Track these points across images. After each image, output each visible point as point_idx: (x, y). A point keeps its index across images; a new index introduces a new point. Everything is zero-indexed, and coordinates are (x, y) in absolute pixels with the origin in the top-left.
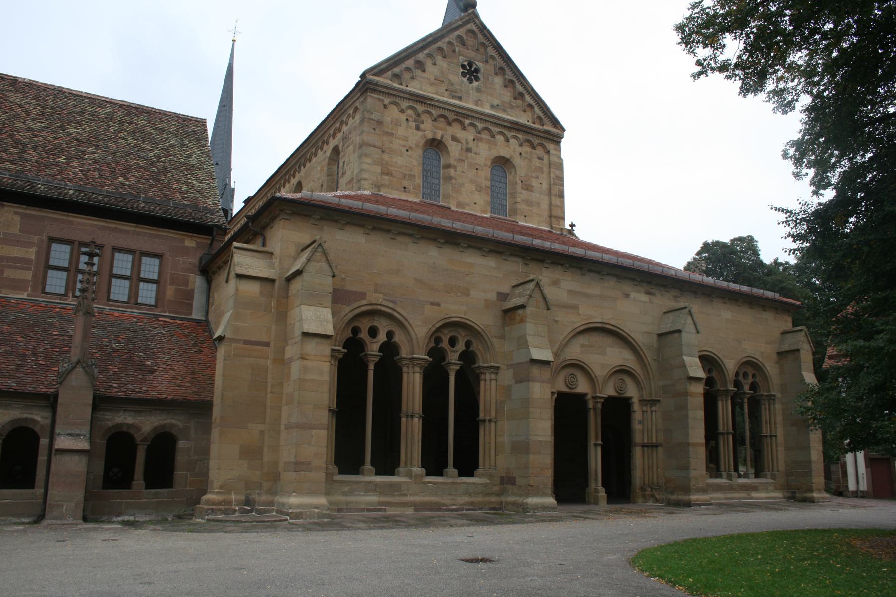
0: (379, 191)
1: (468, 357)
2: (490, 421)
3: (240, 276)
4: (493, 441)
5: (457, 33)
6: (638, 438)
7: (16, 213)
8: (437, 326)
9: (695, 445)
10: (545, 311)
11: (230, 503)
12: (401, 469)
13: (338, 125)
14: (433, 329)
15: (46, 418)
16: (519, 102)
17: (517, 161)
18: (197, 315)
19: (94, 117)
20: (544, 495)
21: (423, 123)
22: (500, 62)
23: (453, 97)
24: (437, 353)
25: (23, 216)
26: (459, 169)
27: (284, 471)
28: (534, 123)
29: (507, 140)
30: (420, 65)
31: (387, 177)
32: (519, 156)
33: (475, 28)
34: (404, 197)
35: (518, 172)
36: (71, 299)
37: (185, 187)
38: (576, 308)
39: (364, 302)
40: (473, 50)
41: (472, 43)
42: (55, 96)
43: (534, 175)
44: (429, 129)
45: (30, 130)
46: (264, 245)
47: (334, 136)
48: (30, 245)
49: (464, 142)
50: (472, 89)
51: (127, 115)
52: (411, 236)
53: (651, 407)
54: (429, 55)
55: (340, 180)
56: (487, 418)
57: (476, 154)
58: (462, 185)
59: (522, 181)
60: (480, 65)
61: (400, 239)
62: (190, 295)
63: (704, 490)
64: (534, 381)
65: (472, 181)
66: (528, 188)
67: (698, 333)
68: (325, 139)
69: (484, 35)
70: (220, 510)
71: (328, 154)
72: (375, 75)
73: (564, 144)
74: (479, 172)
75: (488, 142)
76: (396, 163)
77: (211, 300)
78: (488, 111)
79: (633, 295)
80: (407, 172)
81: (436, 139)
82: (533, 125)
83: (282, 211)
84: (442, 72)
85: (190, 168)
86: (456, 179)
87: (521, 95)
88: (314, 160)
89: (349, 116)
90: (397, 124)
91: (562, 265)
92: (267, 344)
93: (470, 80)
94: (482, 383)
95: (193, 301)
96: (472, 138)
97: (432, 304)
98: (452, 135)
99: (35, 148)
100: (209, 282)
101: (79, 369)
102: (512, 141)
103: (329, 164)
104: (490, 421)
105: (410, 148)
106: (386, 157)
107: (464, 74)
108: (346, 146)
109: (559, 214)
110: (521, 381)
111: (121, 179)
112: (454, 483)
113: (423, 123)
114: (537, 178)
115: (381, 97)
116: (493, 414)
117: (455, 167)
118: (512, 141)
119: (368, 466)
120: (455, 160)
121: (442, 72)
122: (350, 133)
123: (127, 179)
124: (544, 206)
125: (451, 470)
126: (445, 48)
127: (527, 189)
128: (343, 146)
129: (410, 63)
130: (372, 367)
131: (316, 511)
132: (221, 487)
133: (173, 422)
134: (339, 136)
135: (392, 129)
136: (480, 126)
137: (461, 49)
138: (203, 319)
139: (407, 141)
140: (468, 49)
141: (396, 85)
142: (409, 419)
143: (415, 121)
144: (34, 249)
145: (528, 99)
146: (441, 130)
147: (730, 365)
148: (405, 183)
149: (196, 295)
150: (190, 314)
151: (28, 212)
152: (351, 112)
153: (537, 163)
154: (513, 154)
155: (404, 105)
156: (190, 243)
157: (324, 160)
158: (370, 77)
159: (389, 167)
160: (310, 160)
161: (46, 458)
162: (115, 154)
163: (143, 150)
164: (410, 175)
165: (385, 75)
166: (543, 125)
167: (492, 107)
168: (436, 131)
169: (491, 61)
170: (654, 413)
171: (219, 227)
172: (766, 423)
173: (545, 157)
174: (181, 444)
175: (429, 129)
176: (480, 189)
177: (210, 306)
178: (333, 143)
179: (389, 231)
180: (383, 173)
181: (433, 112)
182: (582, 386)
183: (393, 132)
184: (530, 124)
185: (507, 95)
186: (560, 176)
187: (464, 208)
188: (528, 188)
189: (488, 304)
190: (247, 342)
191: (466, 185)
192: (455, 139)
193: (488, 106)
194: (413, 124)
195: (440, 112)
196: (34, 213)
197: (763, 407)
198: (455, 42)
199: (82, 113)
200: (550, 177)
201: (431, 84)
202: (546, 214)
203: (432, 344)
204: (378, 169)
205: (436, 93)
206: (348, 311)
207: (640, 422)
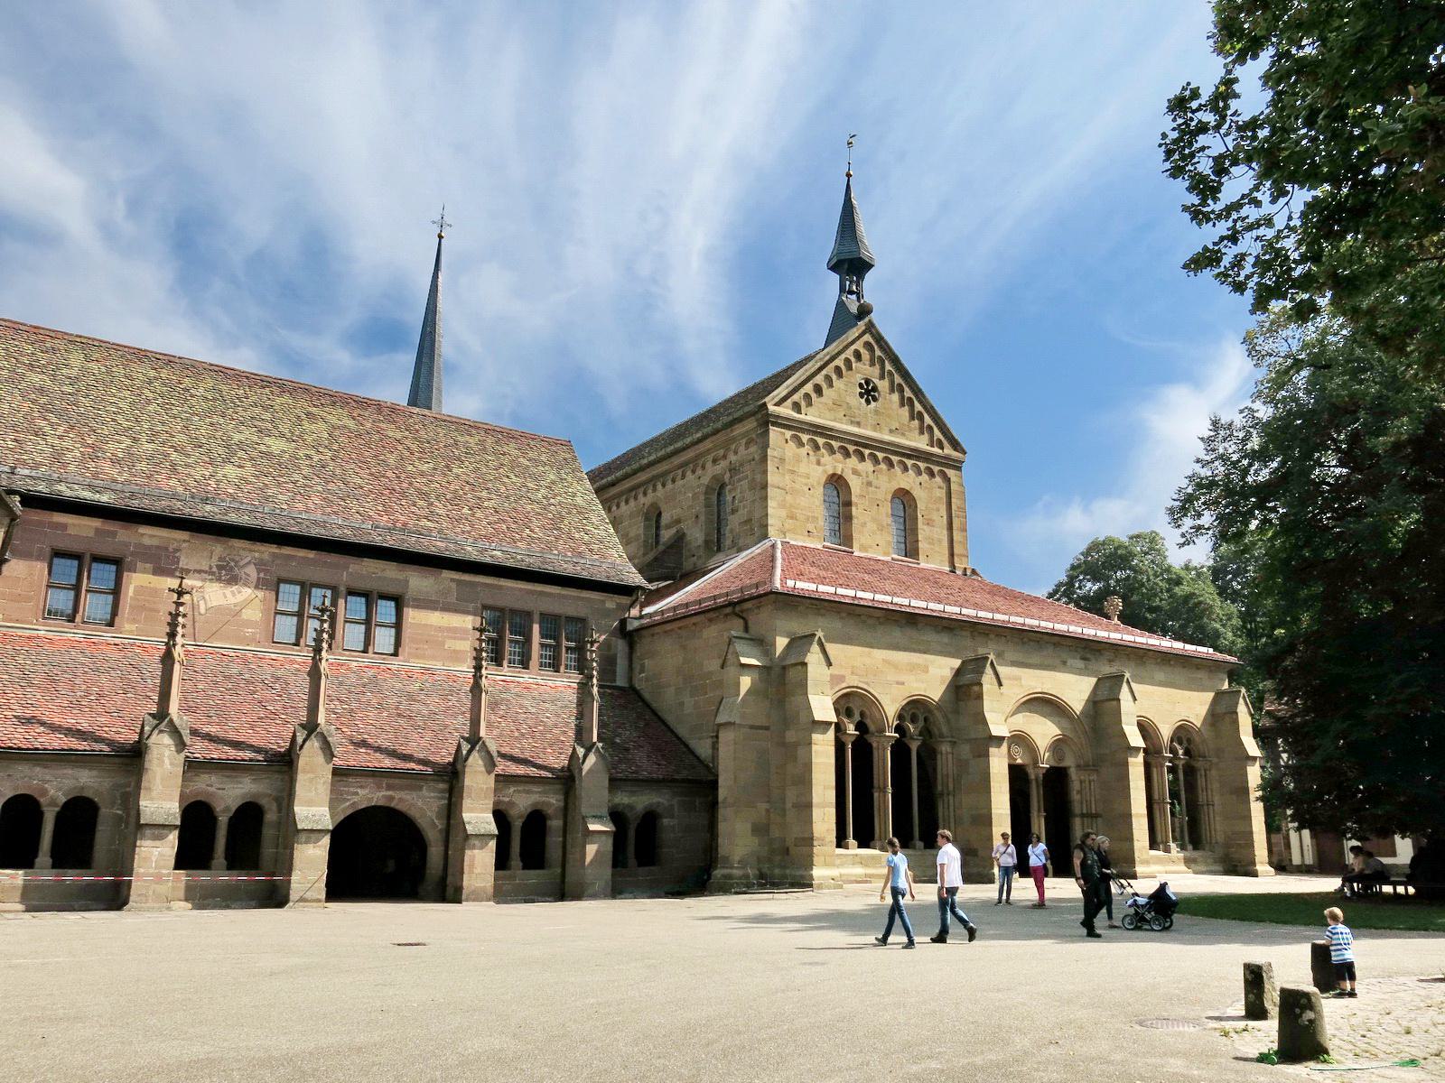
0: (785, 538)
1: (927, 732)
4: (952, 814)
5: (853, 347)
6: (1077, 809)
9: (1137, 815)
11: (747, 876)
12: (878, 844)
13: (721, 452)
15: (559, 801)
17: (917, 493)
18: (621, 681)
23: (852, 423)
27: (795, 846)
28: (932, 446)
30: (818, 390)
32: (919, 486)
33: (871, 340)
36: (506, 669)
37: (586, 537)
38: (1019, 679)
39: (844, 685)
44: (834, 464)
45: (422, 474)
47: (715, 461)
49: (864, 475)
53: (1089, 775)
57: (876, 487)
60: (876, 381)
63: (1146, 862)
64: (994, 756)
65: (874, 520)
66: (929, 523)
69: (881, 347)
70: (742, 883)
71: (706, 480)
72: (775, 405)
74: (880, 508)
76: (799, 504)
77: (637, 667)
78: (887, 437)
79: (1070, 662)
80: (810, 514)
88: (680, 483)
90: (798, 460)
92: (767, 728)
93: (868, 402)
95: (616, 666)
97: (898, 683)
100: (631, 646)
103: (706, 493)
106: (788, 498)
110: (979, 756)
115: (783, 430)
122: (742, 465)
125: (920, 844)
128: (731, 477)
131: (832, 881)
133: (660, 800)
134: (723, 464)
136: (880, 455)
138: (627, 685)
139: (809, 478)
145: (928, 420)
147: (1166, 732)
149: (619, 661)
152: (744, 441)
155: (805, 438)
157: (698, 487)
160: (674, 481)
161: (561, 839)
167: (891, 431)
168: (837, 464)
170: (1092, 784)
172: (1202, 791)
174: (666, 821)
178: (712, 470)
181: (833, 443)
183: (795, 469)
187: (867, 551)
190: (752, 727)
191: (868, 524)
192: (855, 472)
193: (887, 432)
197: (1199, 774)
201: (830, 410)
204: (783, 513)
205: (835, 420)
207: (1078, 792)
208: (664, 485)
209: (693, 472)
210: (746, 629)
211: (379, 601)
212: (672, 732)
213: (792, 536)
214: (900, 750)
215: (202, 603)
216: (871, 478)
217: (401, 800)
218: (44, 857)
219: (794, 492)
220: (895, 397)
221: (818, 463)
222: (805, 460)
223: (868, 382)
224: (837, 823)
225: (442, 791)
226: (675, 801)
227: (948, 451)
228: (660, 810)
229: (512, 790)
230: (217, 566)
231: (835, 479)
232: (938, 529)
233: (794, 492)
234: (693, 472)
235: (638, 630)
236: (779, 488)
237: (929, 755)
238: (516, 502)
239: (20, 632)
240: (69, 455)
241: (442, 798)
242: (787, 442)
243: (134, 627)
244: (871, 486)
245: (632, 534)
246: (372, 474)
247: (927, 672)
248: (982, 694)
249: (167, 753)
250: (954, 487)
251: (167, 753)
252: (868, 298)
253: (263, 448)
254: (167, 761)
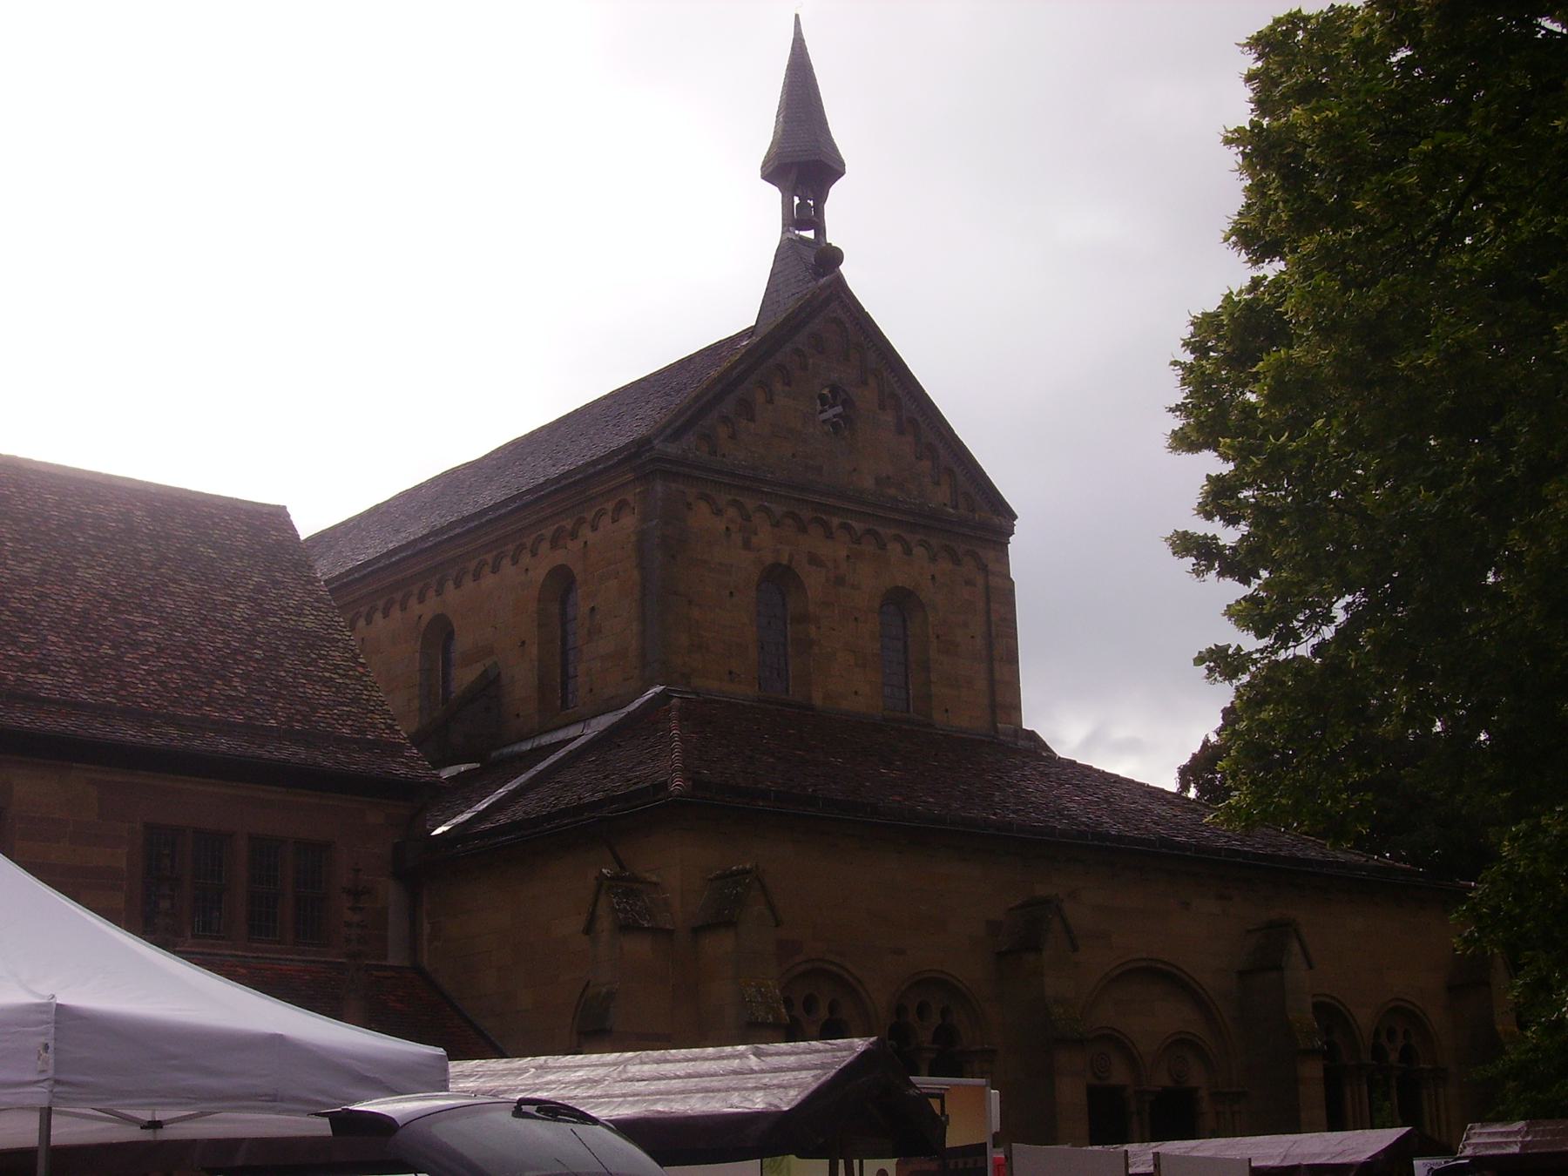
13: (568, 524)
21: (756, 534)
29: (908, 551)
47: (555, 544)
59: (938, 637)
67: (1311, 967)
71: (539, 573)
81: (780, 564)
88: (489, 580)
96: (844, 553)
98: (809, 552)
102: (919, 551)
113: (756, 534)
118: (919, 551)
152: (610, 506)
168: (779, 546)
178: (549, 559)
182: (1119, 1075)
192: (814, 560)
208: (458, 584)
209: (515, 562)
221: (747, 545)
223: (834, 389)
252: (832, 238)
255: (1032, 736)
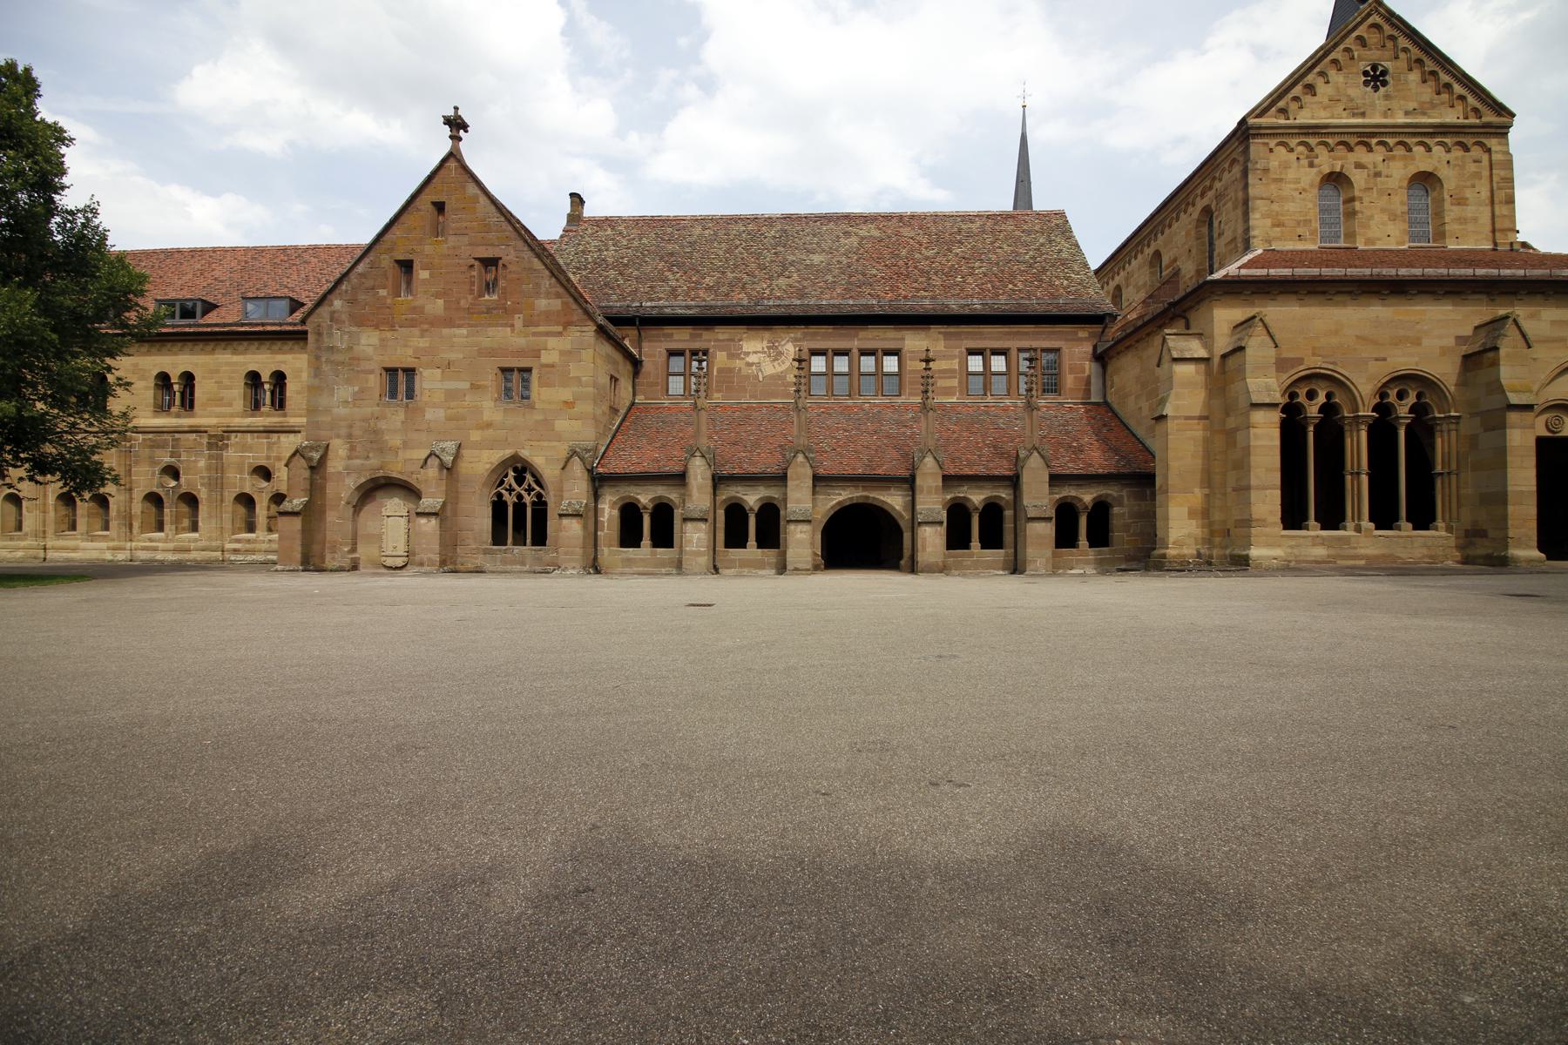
2: (1449, 474)
3: (1176, 360)
5: (1354, 35)
7: (940, 333)
8: (1384, 380)
10: (1526, 351)
12: (1350, 524)
13: (1208, 183)
14: (1380, 385)
16: (1445, 96)
17: (1444, 173)
19: (970, 234)
20: (1529, 547)
22: (1416, 52)
23: (1354, 115)
24: (1383, 408)
25: (945, 334)
26: (1366, 200)
28: (1466, 118)
29: (1429, 150)
30: (1310, 88)
31: (1278, 229)
32: (1446, 166)
34: (1300, 246)
35: (1445, 186)
37: (1065, 282)
39: (1301, 368)
40: (1378, 49)
41: (1375, 40)
42: (935, 222)
43: (1469, 183)
44: (1326, 162)
45: (927, 258)
46: (1188, 327)
47: (1203, 195)
48: (952, 357)
49: (1371, 166)
50: (1379, 99)
51: (995, 224)
52: (1350, 293)
54: (1322, 74)
55: (1217, 243)
56: (1447, 470)
58: (1371, 217)
61: (1338, 298)
62: (1088, 382)
64: (1511, 428)
65: (1383, 210)
66: (1461, 202)
68: (1191, 200)
69: (1393, 25)
71: (1196, 215)
72: (1256, 117)
73: (1513, 134)
74: (1392, 197)
75: (1404, 158)
77: (1109, 383)
78: (1401, 120)
82: (1466, 121)
83: (1212, 293)
84: (1338, 89)
85: (1064, 263)
86: (1362, 213)
87: (1448, 86)
88: (1175, 225)
89: (1224, 170)
90: (1285, 166)
91: (1543, 293)
93: (1376, 89)
94: (1438, 434)
96: (1381, 159)
99: (936, 274)
100: (1104, 367)
101: (1036, 454)
103: (1197, 227)
104: (1449, 474)
105: (1304, 190)
106: (1275, 207)
107: (1366, 83)
108: (1221, 204)
109: (1507, 224)
110: (1494, 429)
111: (1010, 286)
112: (1408, 537)
114: (1473, 186)
115: (1266, 141)
116: (1454, 466)
117: (1361, 199)
119: (1312, 522)
120: (1360, 190)
121: (1338, 89)
122: (1226, 189)
123: (1015, 286)
124: (1485, 218)
125: (1406, 527)
126: (1340, 58)
127: (1459, 204)
129: (1297, 91)
130: (1311, 428)
132: (1174, 543)
133: (1109, 492)
134: (1210, 194)
135: (1281, 173)
136: (1391, 141)
137: (1362, 52)
140: (1370, 49)
141: (1282, 121)
142: (1355, 476)
143: (1307, 157)
144: (957, 360)
145: (1458, 89)
146: (1341, 159)
148: (1300, 231)
149: (1093, 380)
150: (1089, 398)
151: (948, 330)
152: (1226, 165)
153: (1472, 167)
154: (1437, 164)
155: (1293, 142)
156: (1083, 333)
157: (1190, 223)
158: (1251, 121)
159: (1280, 217)
160: (1170, 226)
162: (997, 264)
163: (1018, 254)
164: (1305, 220)
165: (1269, 113)
166: (1480, 117)
167: (1407, 113)
169: (1402, 56)
171: (1110, 315)
173: (1485, 157)
174: (1116, 510)
175: (1326, 162)
176: (1393, 217)
177: (1108, 389)
179: (1324, 293)
180: (1274, 225)
181: (1330, 141)
183: (1283, 176)
184: (1461, 121)
185: (1427, 92)
186: (1508, 176)
187: (1374, 244)
188: (1461, 202)
189: (1444, 351)
190: (1187, 418)
191: (1376, 216)
192: (1359, 166)
193: (1401, 113)
194: (1305, 162)
195: (1338, 139)
196: (952, 330)
198: (1353, 47)
199: (960, 231)
200: (1491, 181)
201: (1325, 109)
202: (1488, 228)
203: (1378, 400)
204: (1269, 222)
205: (1332, 117)
206: (1287, 378)
209: (1185, 212)
210: (1188, 327)
211: (885, 358)
212: (1134, 435)
213: (1280, 243)
214: (1382, 429)
215: (760, 374)
216: (1381, 167)
217: (874, 498)
218: (646, 541)
219: (1282, 199)
220: (1414, 76)
221: (1311, 165)
222: (1295, 164)
224: (1282, 505)
225: (906, 490)
226: (1124, 493)
227: (1490, 117)
228: (1109, 500)
229: (965, 488)
230: (768, 347)
231: (1334, 177)
232: (1473, 208)
233: (1282, 199)
234: (1185, 212)
235: (1105, 351)
236: (1262, 199)
237: (1423, 430)
238: (1004, 265)
239: (653, 406)
240: (680, 290)
241: (908, 495)
242: (1271, 151)
243: (719, 395)
244: (1380, 176)
245: (1141, 283)
246: (886, 266)
247: (1420, 344)
248: (1499, 359)
249: (699, 471)
250: (1495, 157)
251: (699, 471)
253: (808, 262)
254: (699, 477)
255: (1524, 245)
